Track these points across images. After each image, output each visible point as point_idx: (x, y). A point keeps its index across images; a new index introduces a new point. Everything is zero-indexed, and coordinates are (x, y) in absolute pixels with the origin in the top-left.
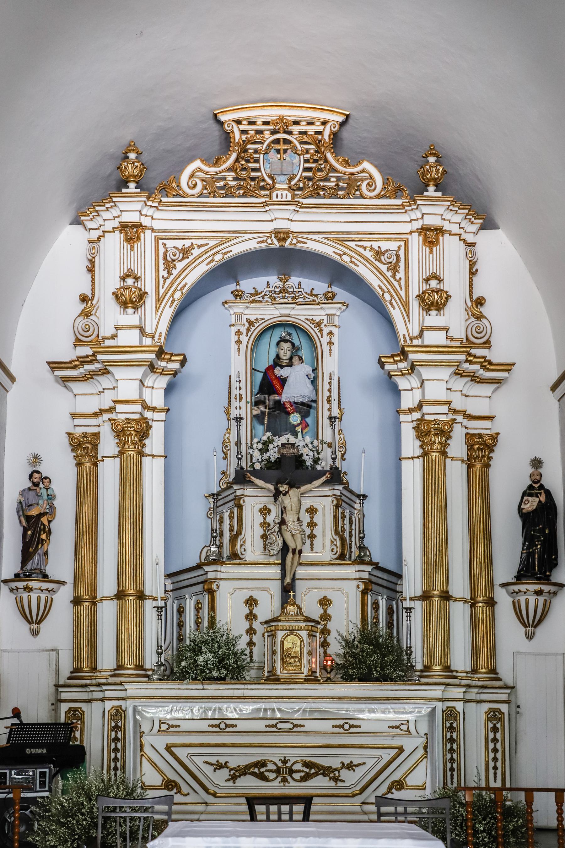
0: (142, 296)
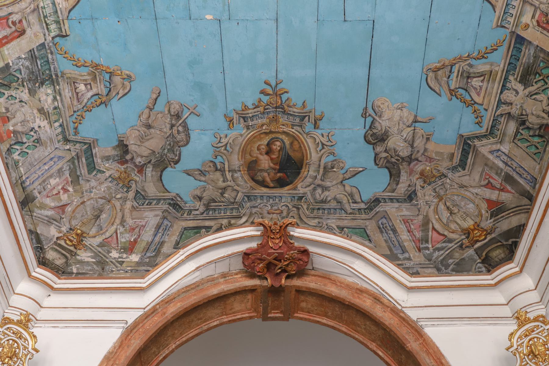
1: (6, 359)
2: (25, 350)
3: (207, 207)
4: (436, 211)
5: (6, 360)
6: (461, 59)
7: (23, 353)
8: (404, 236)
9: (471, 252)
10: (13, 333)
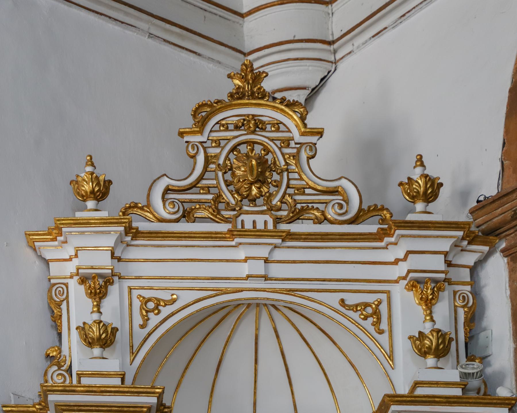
1: (250, 189)
2: (288, 146)
5: (255, 191)
7: (283, 155)
10: (237, 128)
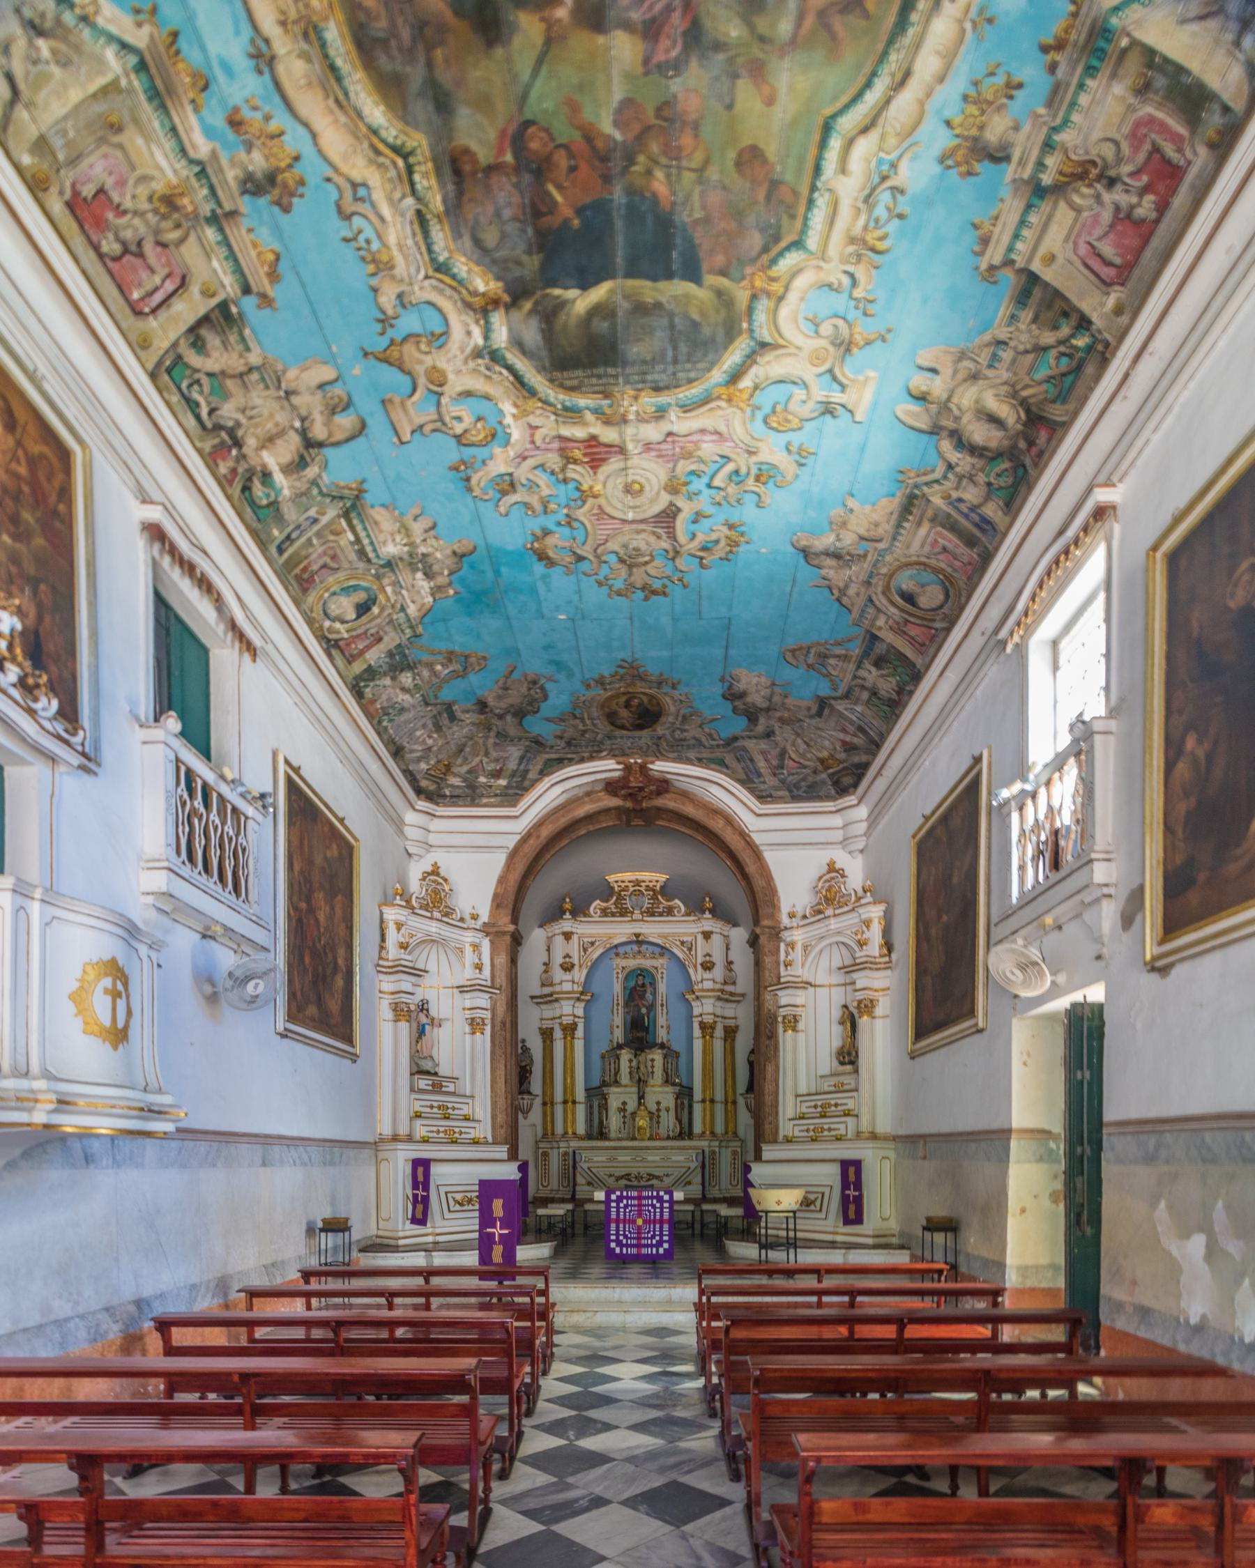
0: (573, 966)
3: (569, 744)
4: (793, 745)
6: (818, 644)
8: (761, 764)
9: (824, 776)
